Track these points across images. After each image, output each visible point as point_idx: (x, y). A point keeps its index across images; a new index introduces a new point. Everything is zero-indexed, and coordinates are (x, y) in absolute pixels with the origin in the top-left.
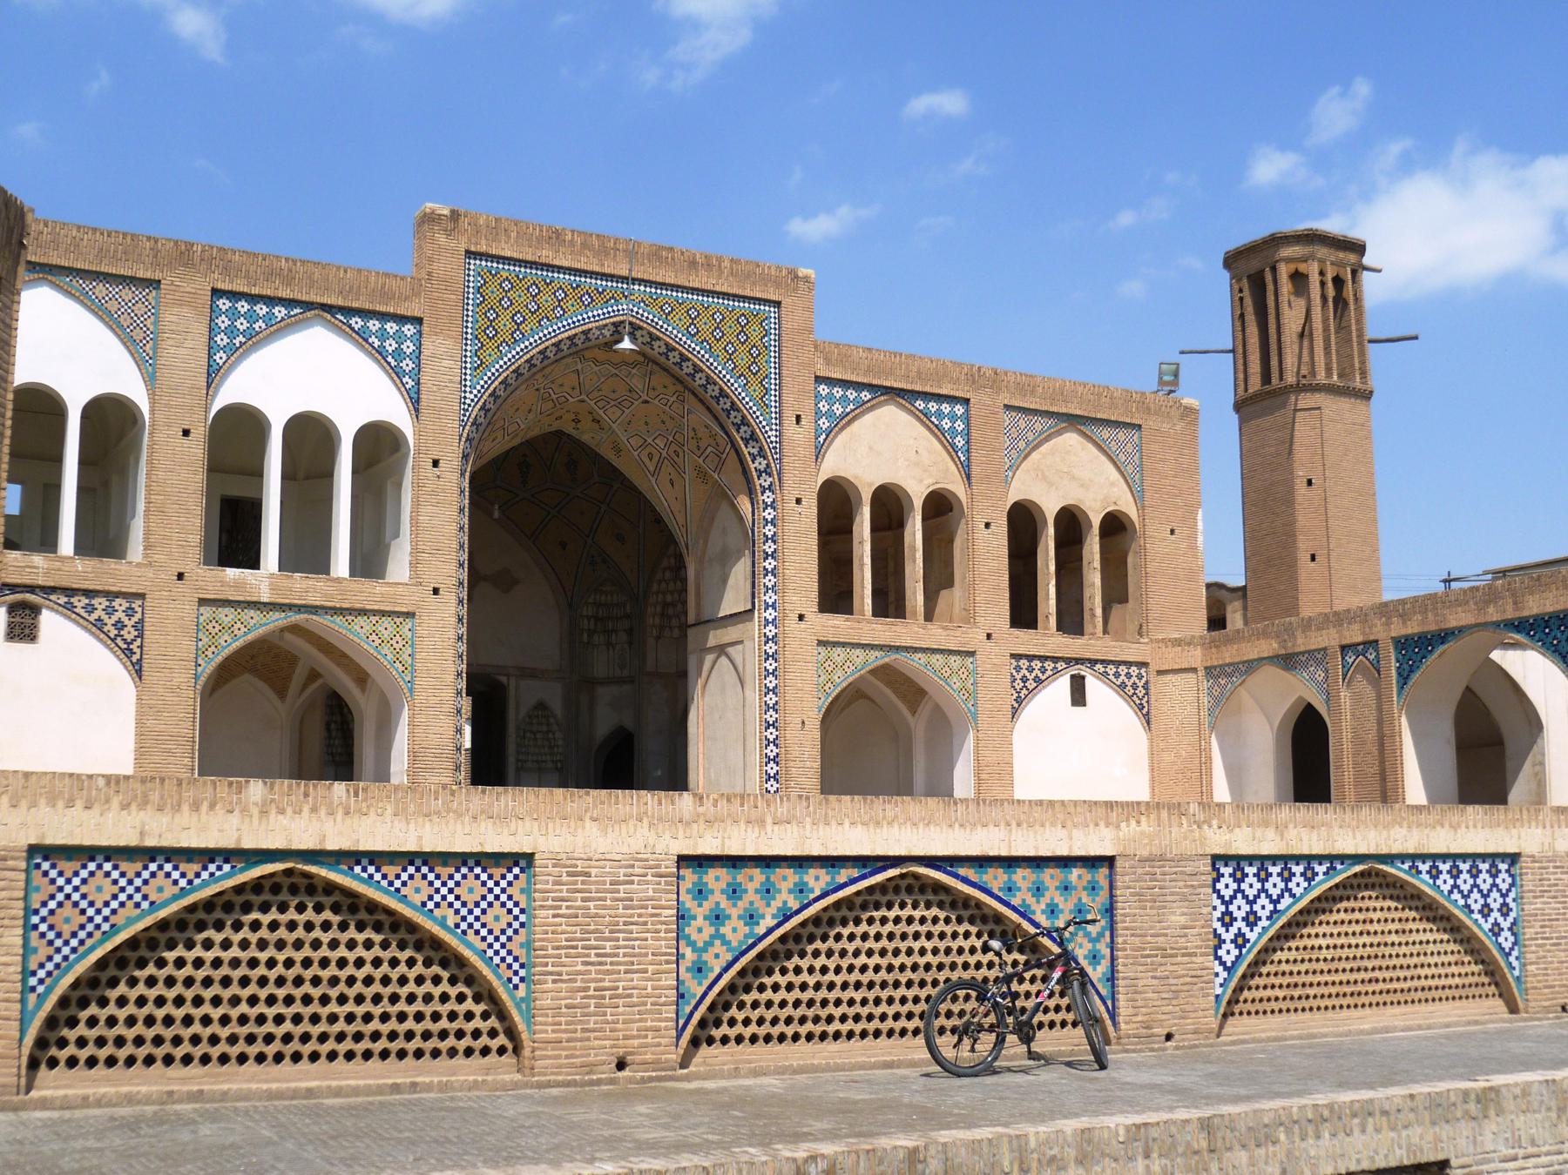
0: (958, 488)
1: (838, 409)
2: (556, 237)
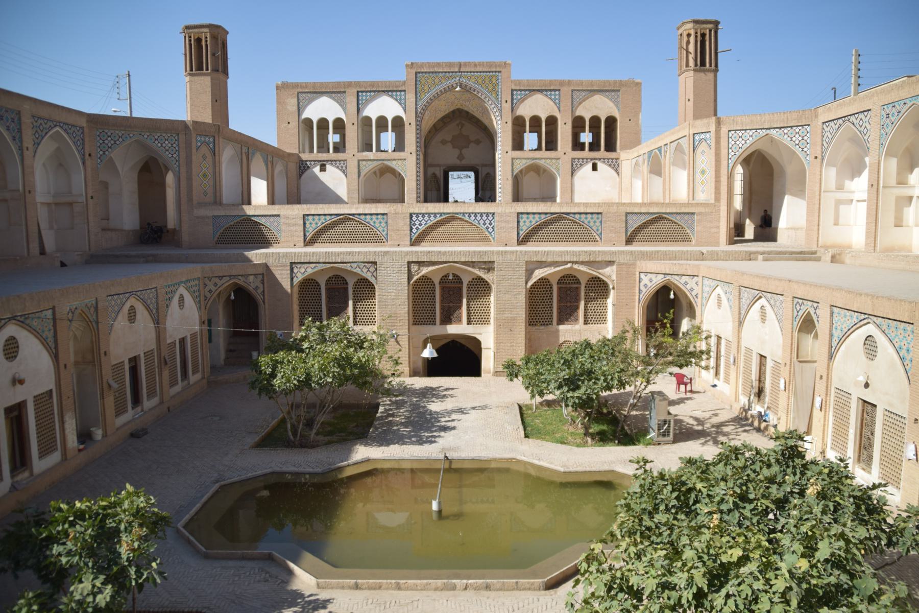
2: (438, 64)
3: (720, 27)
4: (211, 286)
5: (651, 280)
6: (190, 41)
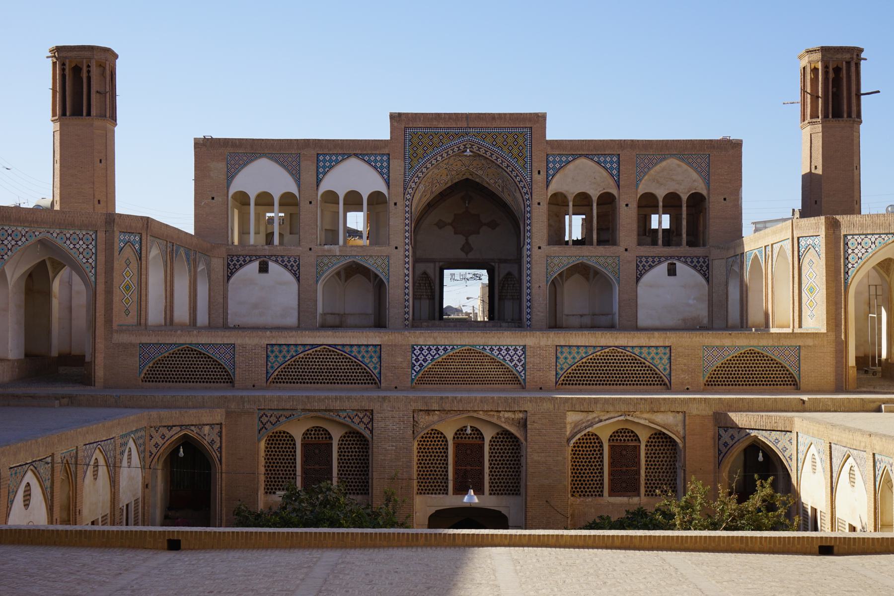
0: (614, 192)
1: (558, 166)
3: (863, 55)
4: (158, 439)
5: (732, 437)
6: (63, 70)
